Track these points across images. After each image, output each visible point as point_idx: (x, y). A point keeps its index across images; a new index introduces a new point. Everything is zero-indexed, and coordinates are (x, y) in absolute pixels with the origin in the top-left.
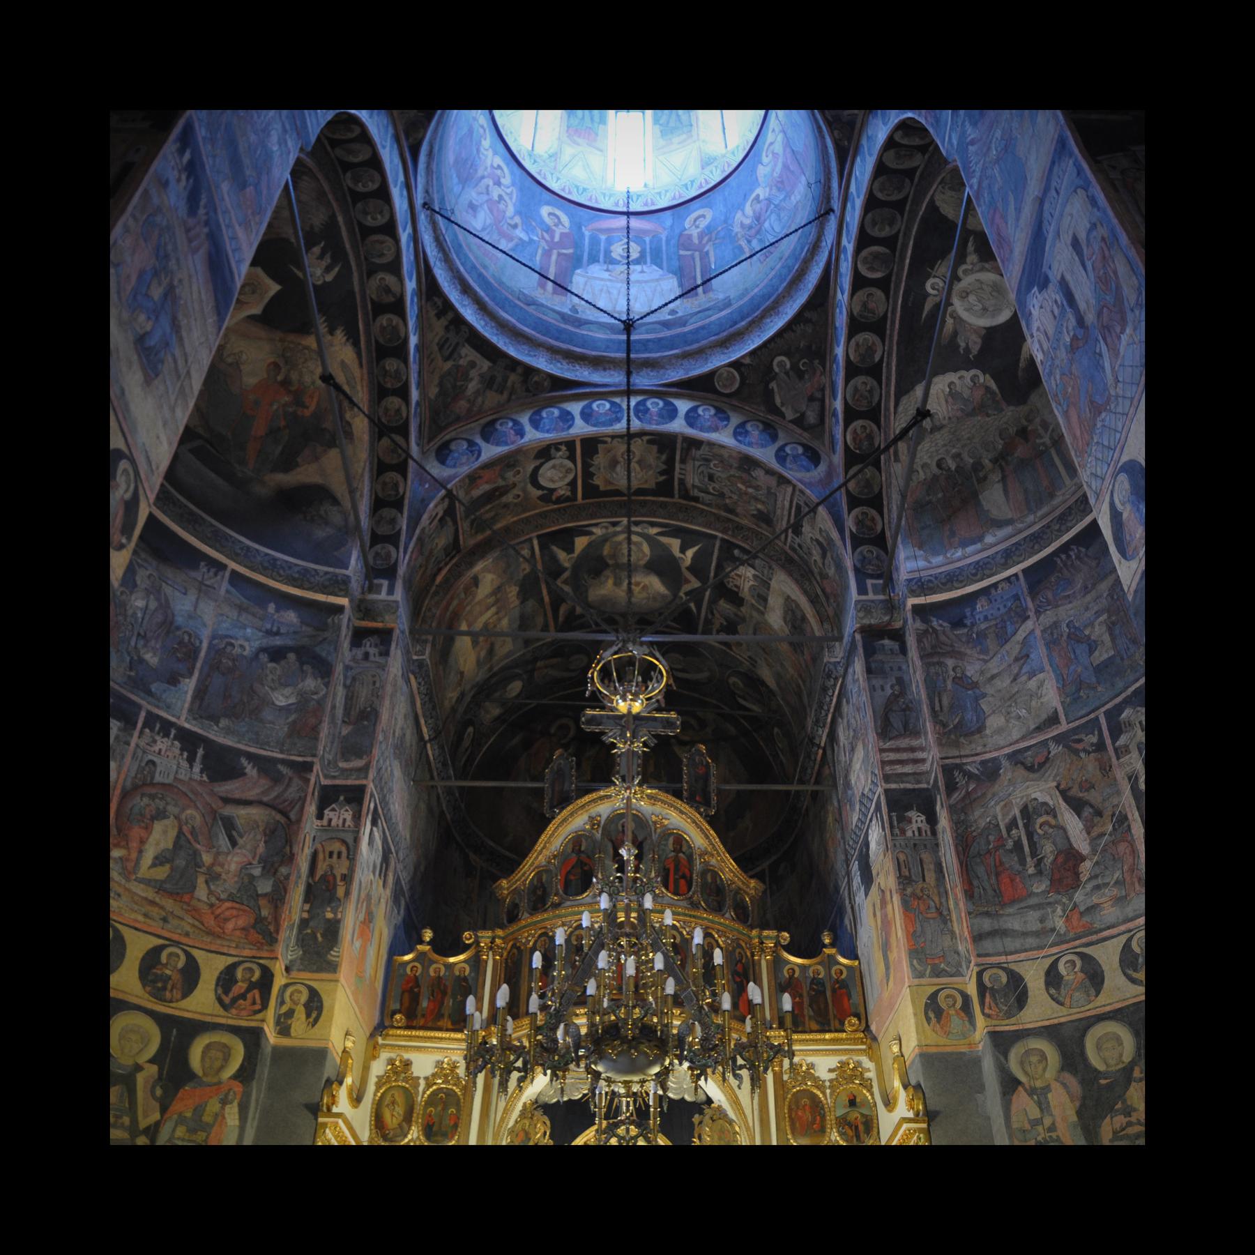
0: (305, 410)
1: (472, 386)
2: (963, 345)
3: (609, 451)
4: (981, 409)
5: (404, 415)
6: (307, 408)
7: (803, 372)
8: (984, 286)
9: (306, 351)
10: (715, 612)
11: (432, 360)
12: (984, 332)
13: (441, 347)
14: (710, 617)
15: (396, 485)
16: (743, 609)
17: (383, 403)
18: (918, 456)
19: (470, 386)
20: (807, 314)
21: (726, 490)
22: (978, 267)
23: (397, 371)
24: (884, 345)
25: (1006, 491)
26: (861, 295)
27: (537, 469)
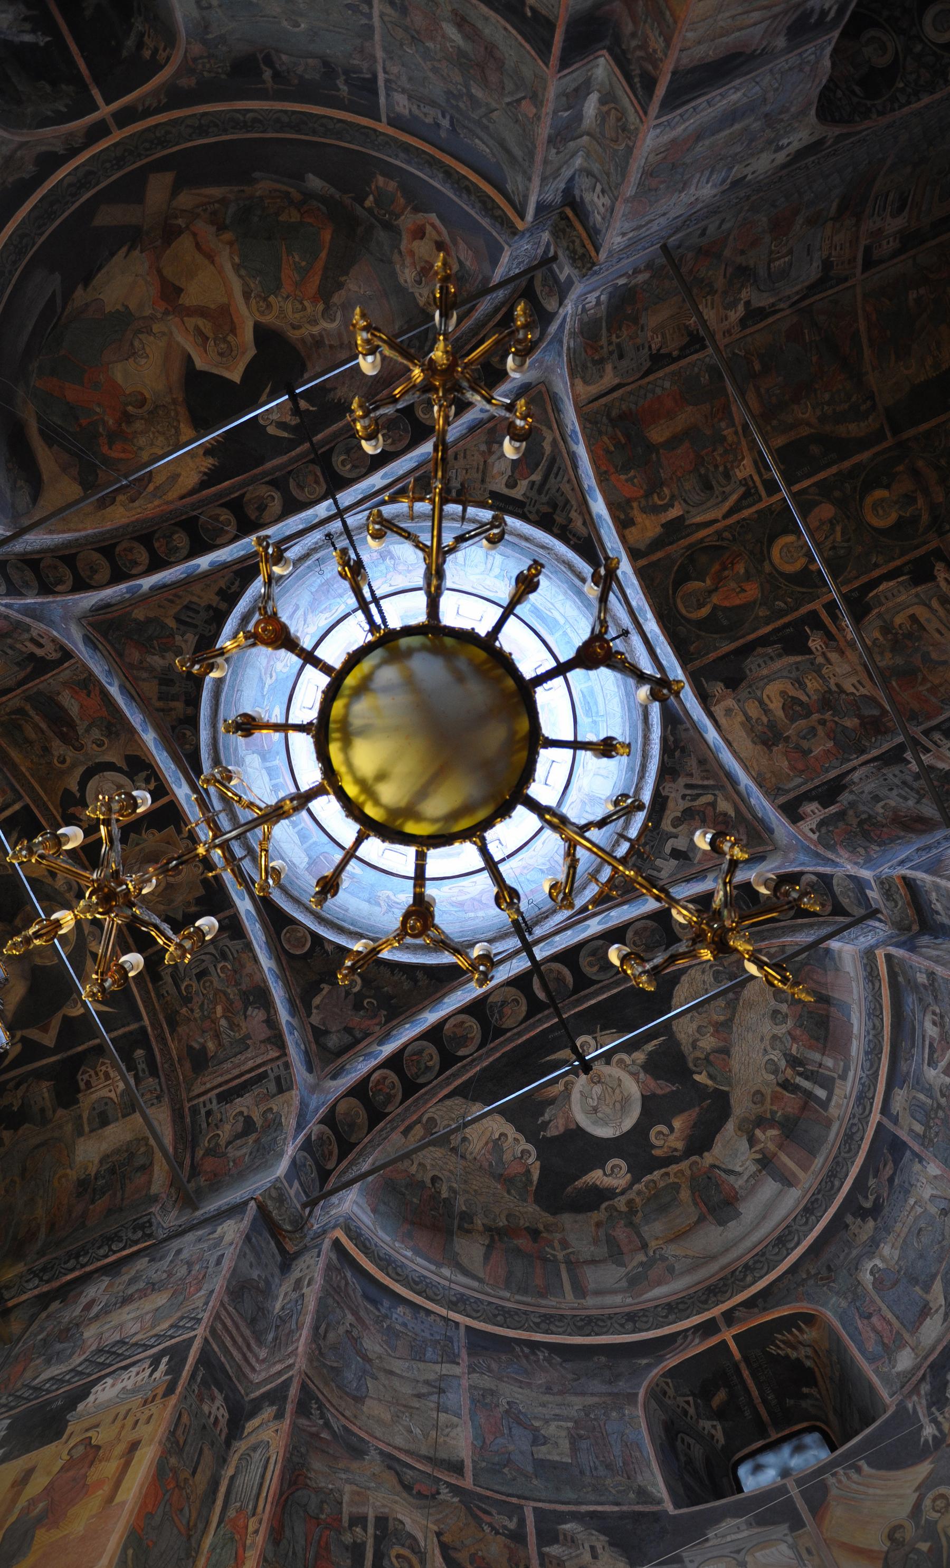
0: (106, 447)
1: (156, 661)
2: (547, 1117)
3: (168, 843)
4: (508, 1181)
5: (134, 572)
6: (110, 448)
7: (363, 1008)
8: (617, 1091)
9: (173, 431)
10: (23, 1087)
11: (172, 601)
12: (573, 1126)
13: (187, 607)
14: (11, 1084)
15: (60, 582)
16: (60, 1112)
17: (136, 544)
18: (424, 1152)
19: (156, 658)
20: (420, 975)
21: (197, 1000)
22: (634, 1069)
23: (177, 549)
24: (477, 1051)
25: (487, 1257)
26: (513, 992)
27: (111, 767)
